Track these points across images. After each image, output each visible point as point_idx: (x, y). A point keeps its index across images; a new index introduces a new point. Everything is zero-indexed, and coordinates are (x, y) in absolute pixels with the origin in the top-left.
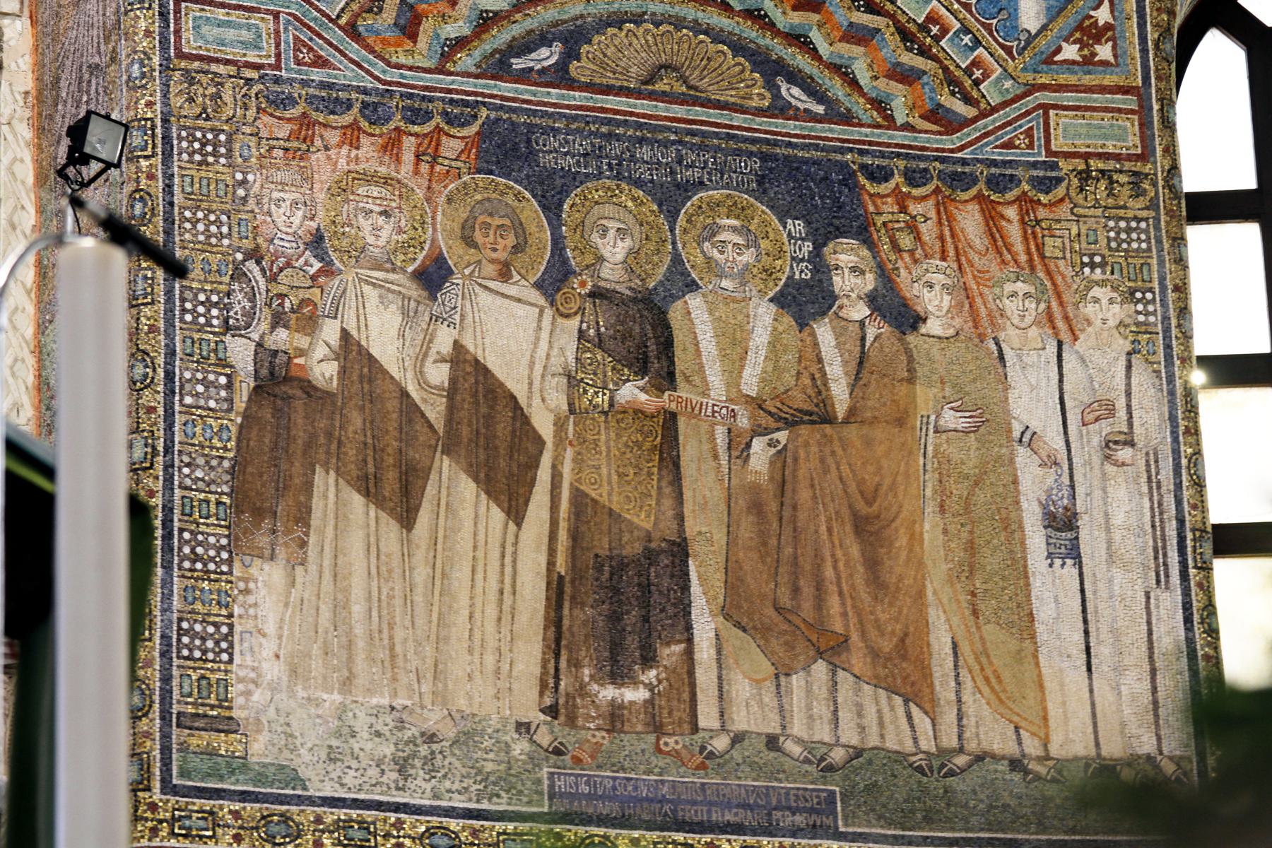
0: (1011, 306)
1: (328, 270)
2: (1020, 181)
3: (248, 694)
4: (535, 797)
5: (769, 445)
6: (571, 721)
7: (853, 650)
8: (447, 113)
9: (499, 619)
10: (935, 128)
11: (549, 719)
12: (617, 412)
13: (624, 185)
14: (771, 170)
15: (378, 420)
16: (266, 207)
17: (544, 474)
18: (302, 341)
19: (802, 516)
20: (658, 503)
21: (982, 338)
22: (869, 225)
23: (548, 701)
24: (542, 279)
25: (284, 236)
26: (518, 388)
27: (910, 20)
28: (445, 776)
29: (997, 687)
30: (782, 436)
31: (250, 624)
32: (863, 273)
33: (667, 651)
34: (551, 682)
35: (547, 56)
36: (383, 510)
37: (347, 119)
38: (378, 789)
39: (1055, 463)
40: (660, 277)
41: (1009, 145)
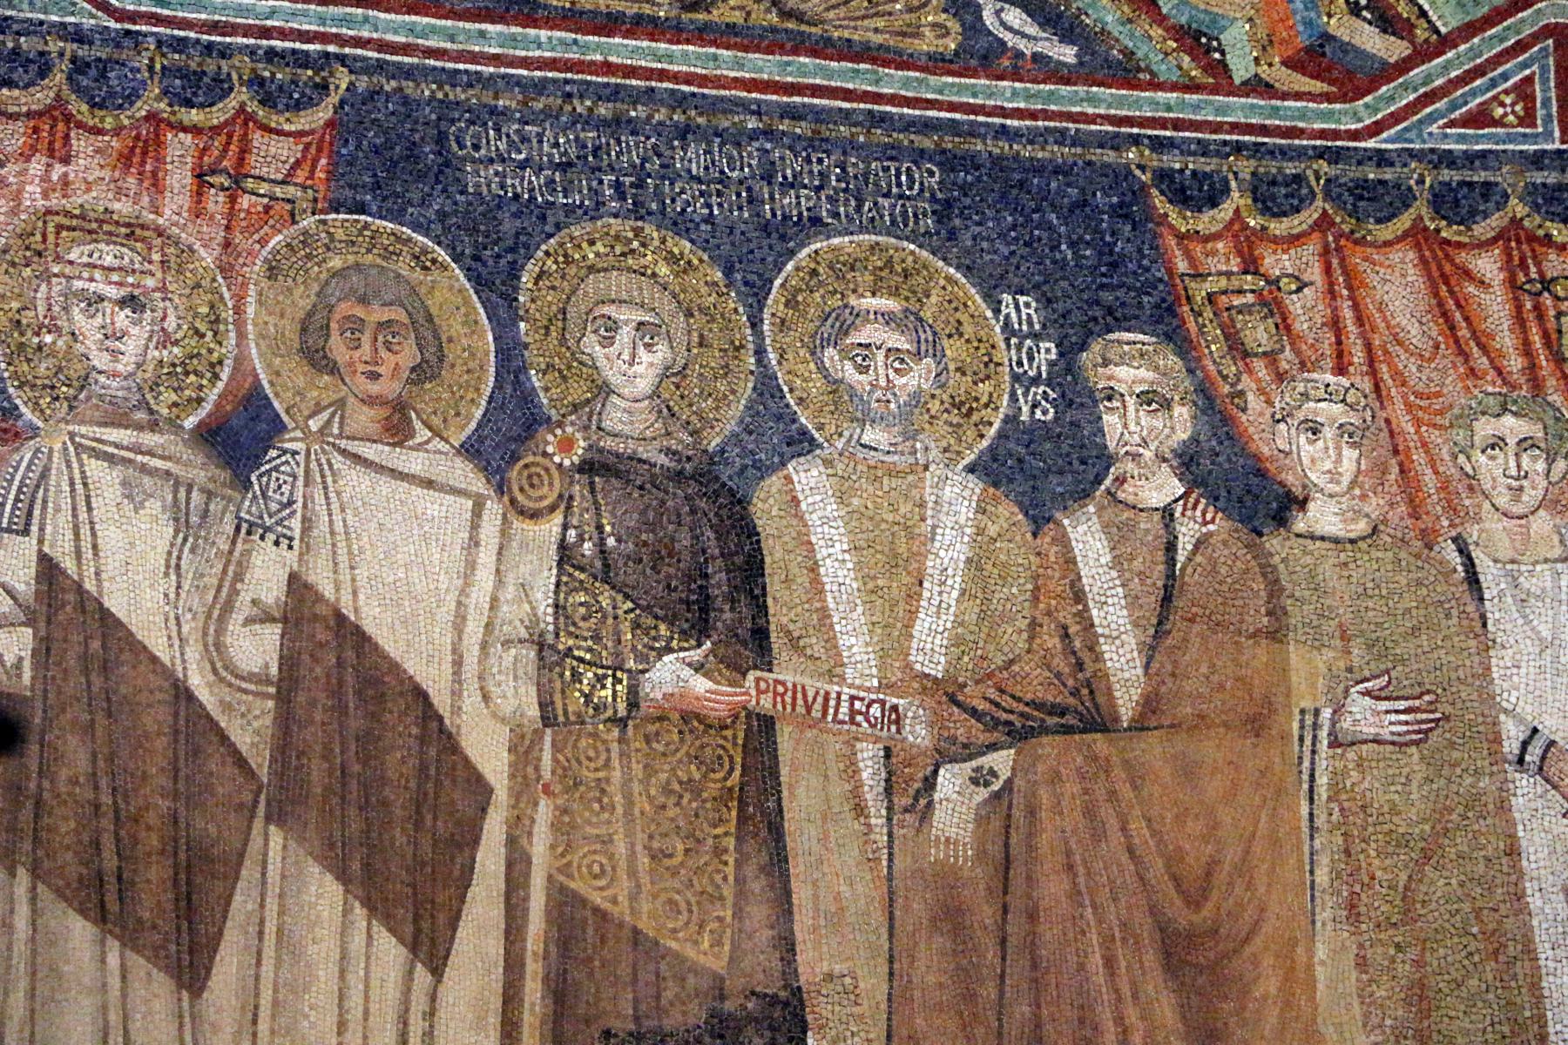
0: (1490, 468)
2: (1506, 196)
5: (975, 781)
8: (262, 82)
10: (1318, 86)
13: (650, 230)
14: (964, 189)
15: (124, 753)
17: (490, 859)
19: (1049, 933)
20: (738, 913)
26: (433, 677)
30: (1002, 761)
32: (1167, 405)
37: (40, 97)
40: (731, 426)
41: (1480, 118)
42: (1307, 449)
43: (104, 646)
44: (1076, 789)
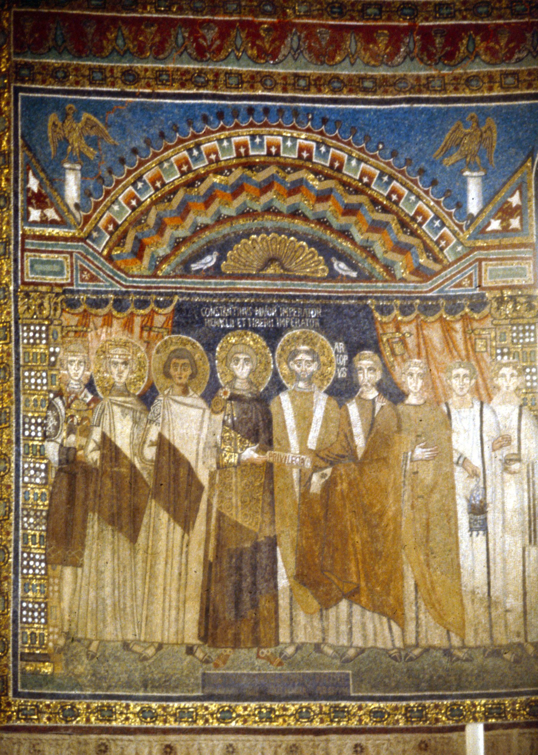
0: (456, 383)
2: (464, 307)
7: (362, 592)
10: (417, 279)
17: (203, 506)
18: (83, 441)
21: (438, 403)
27: (407, 215)
35: (210, 260)
40: (266, 385)
42: (409, 380)
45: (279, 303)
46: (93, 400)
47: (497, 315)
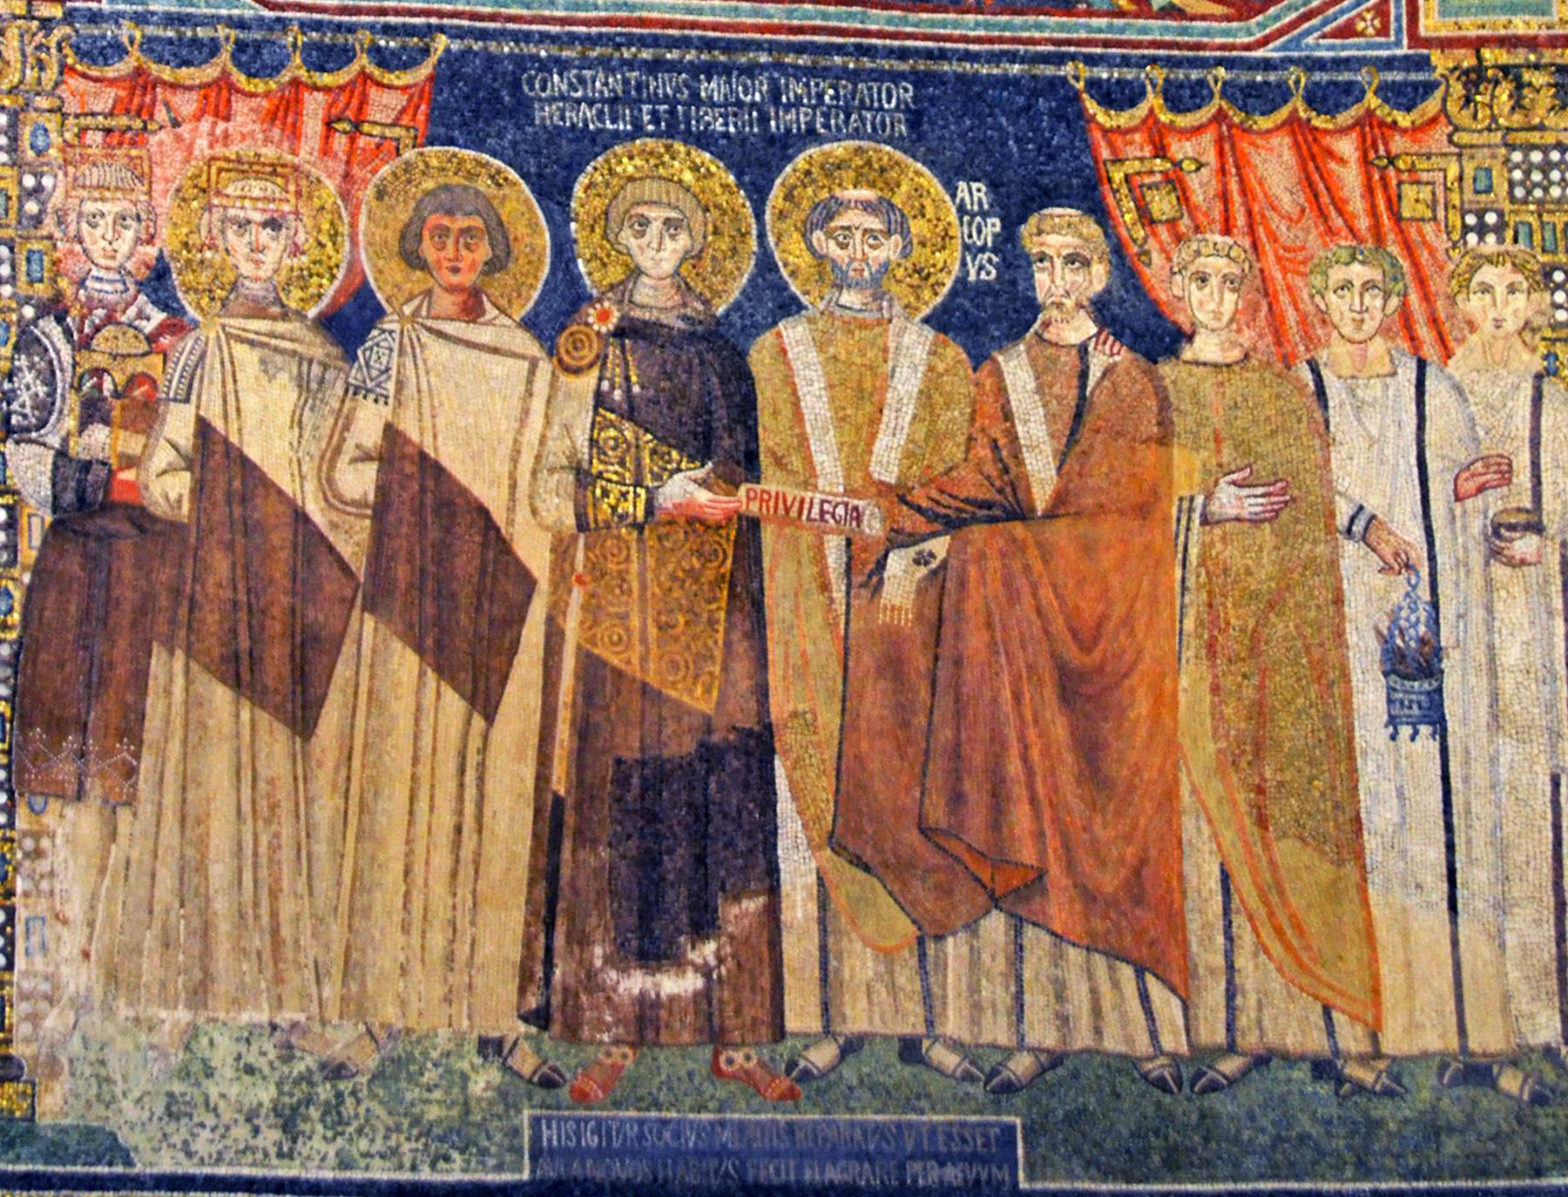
0: (1339, 305)
1: (177, 324)
3: (35, 1018)
4: (508, 1158)
5: (917, 562)
6: (572, 1033)
7: (1053, 894)
9: (454, 874)
11: (534, 1030)
12: (659, 524)
13: (679, 147)
14: (933, 101)
15: (256, 564)
16: (72, 230)
17: (533, 633)
18: (132, 444)
19: (970, 676)
20: (725, 669)
21: (1288, 361)
22: (1099, 182)
23: (533, 1002)
24: (535, 313)
25: (102, 274)
26: (494, 500)
28: (360, 1131)
29: (1295, 943)
30: (939, 546)
31: (42, 906)
32: (1086, 263)
33: (735, 910)
34: (539, 973)
36: (263, 708)
37: (210, 72)
38: (250, 1158)
39: (1408, 566)
40: (736, 295)
42: (1195, 294)
43: (244, 483)
44: (998, 564)
45: (779, 66)
46: (162, 329)
47: (1464, 118)
